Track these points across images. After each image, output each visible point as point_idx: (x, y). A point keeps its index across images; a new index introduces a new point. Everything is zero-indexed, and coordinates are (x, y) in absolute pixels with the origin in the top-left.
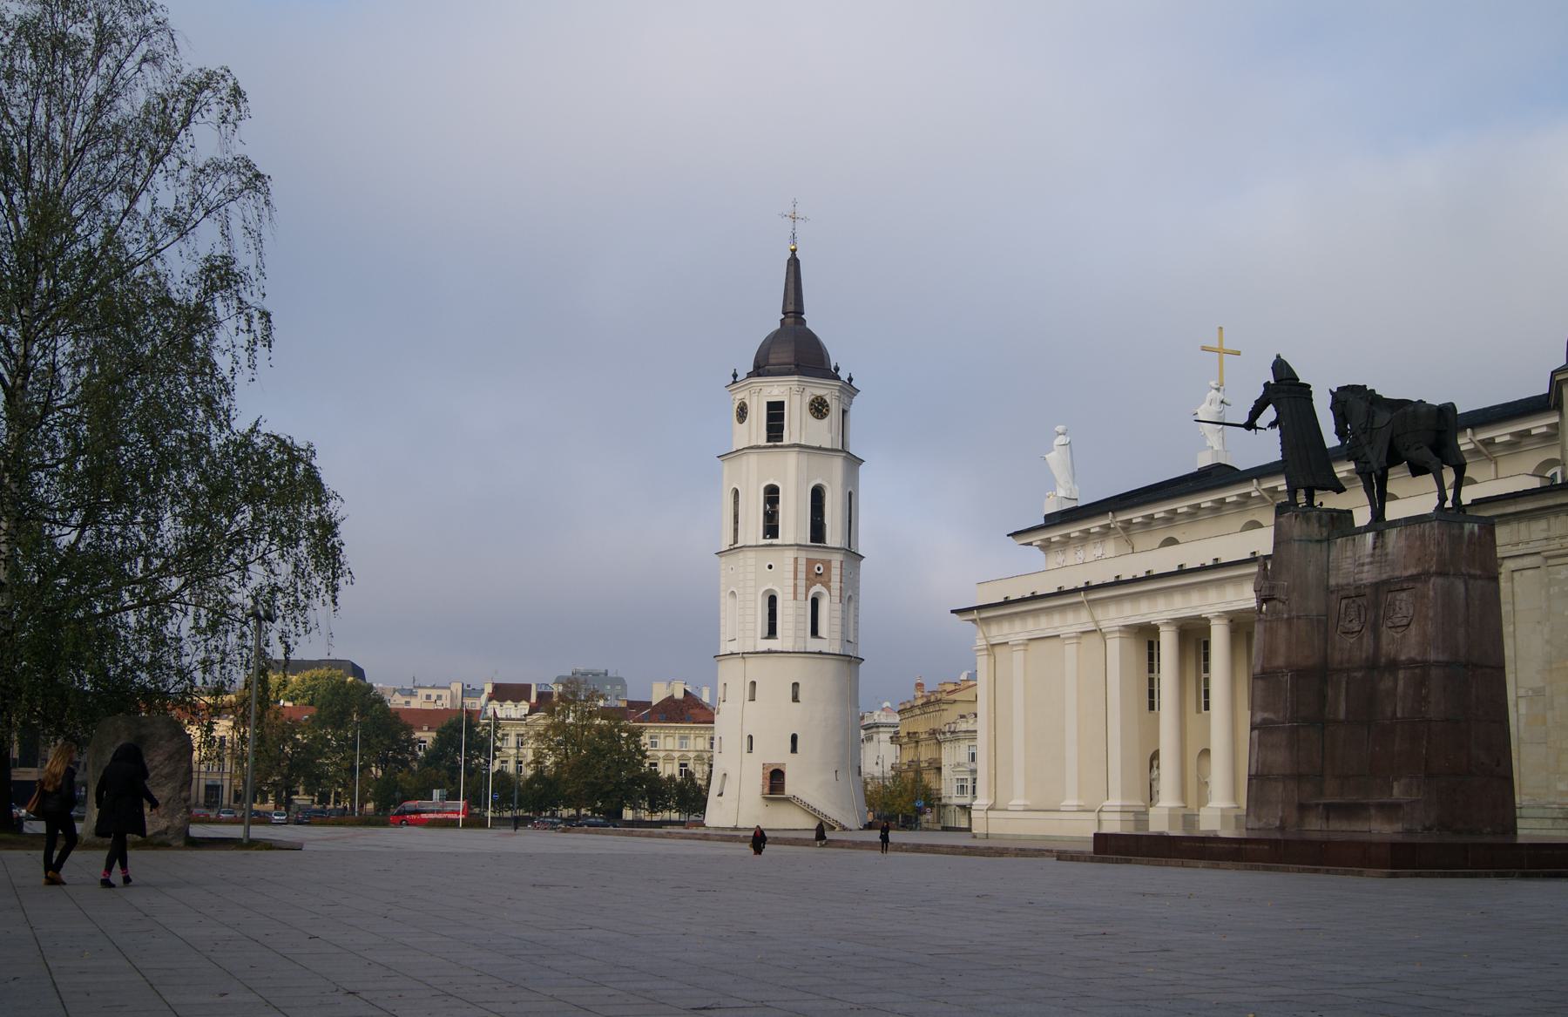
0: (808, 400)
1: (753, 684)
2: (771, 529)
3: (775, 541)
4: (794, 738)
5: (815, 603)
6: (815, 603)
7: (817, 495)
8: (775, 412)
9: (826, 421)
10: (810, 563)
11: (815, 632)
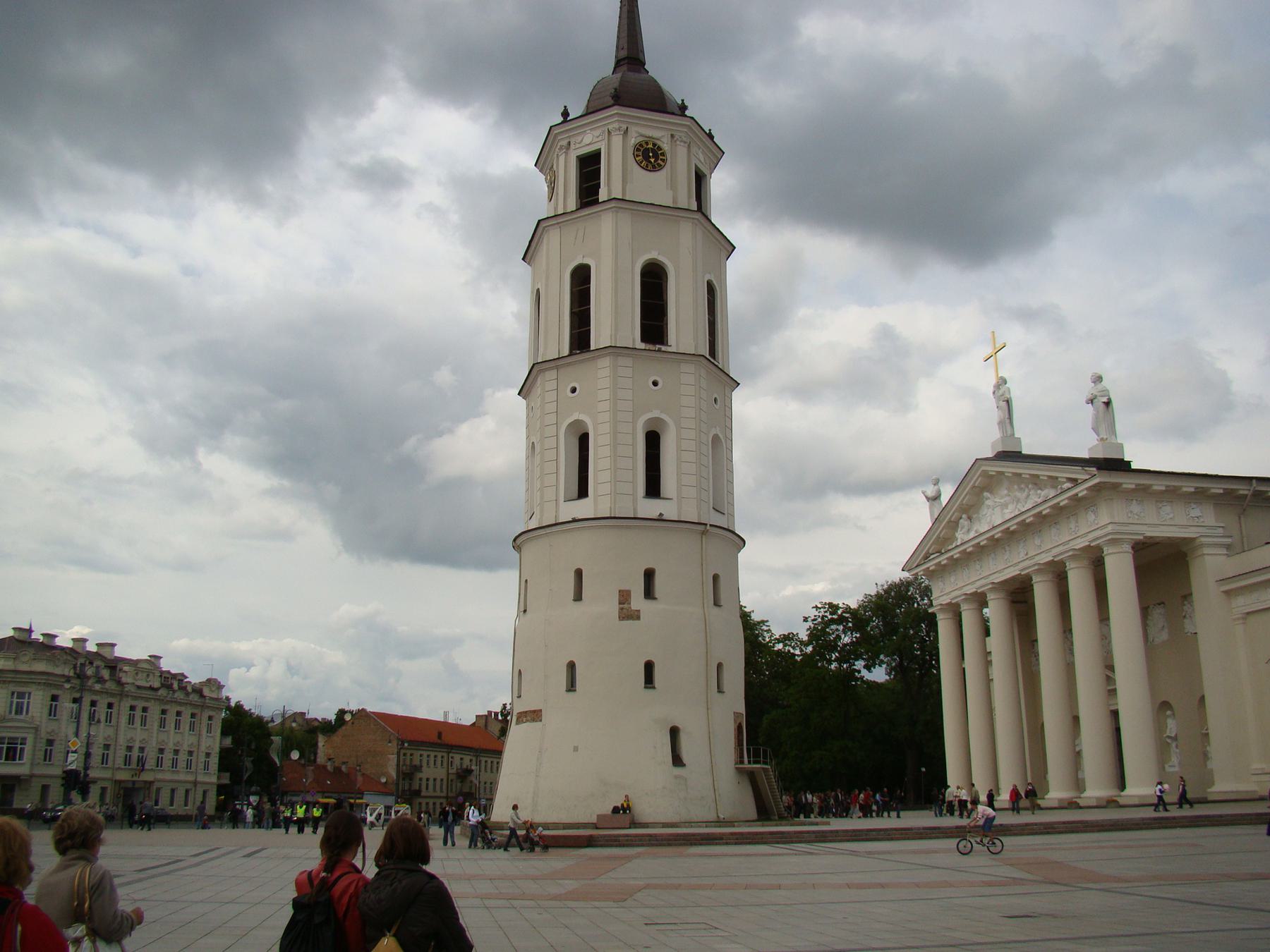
0: (633, 141)
7: (654, 282)
8: (589, 166)
11: (653, 488)
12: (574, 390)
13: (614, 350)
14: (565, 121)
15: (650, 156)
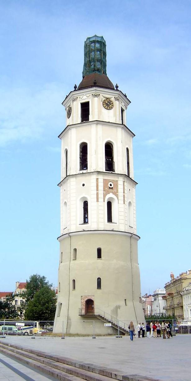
1: (75, 250)
2: (84, 164)
3: (84, 171)
4: (99, 281)
5: (109, 204)
6: (109, 204)
8: (85, 107)
9: (112, 111)
10: (105, 181)
14: (75, 90)
15: (108, 104)
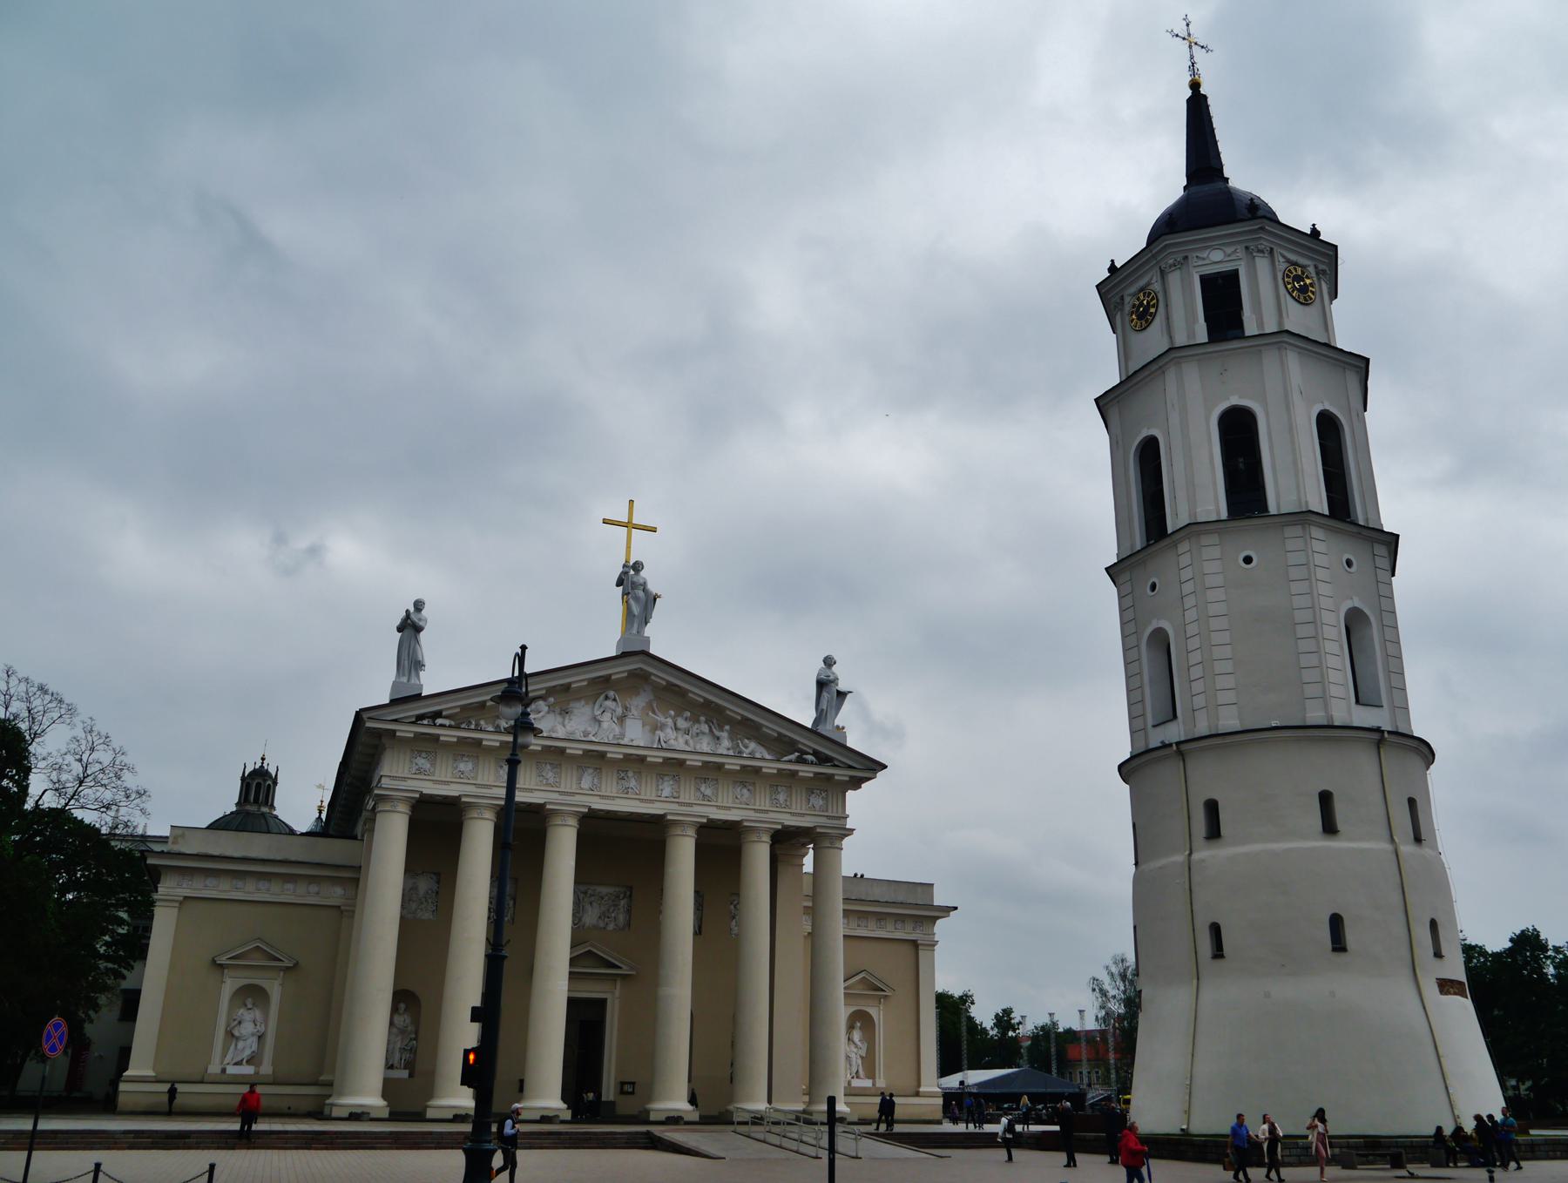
12: (1248, 560)
13: (1304, 517)
